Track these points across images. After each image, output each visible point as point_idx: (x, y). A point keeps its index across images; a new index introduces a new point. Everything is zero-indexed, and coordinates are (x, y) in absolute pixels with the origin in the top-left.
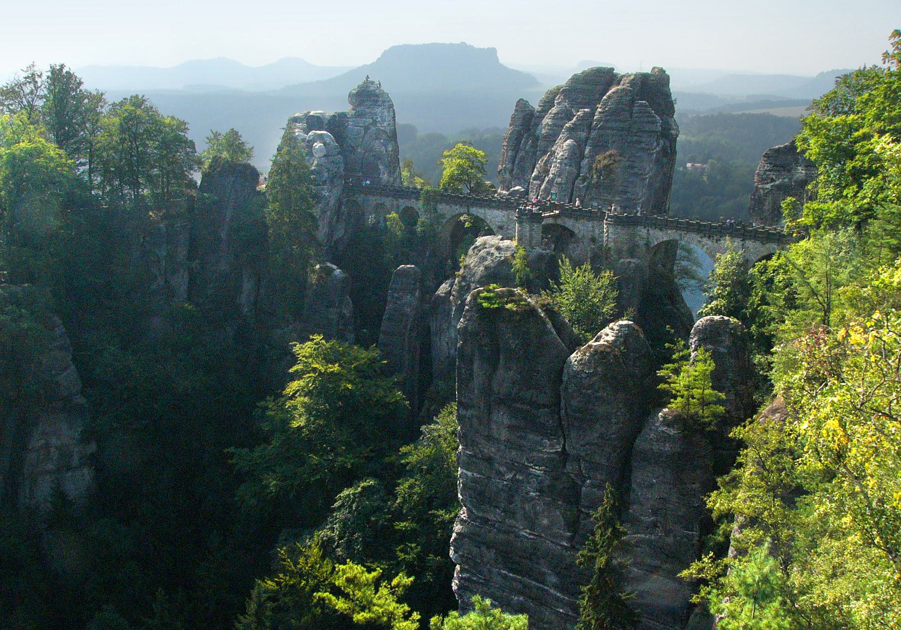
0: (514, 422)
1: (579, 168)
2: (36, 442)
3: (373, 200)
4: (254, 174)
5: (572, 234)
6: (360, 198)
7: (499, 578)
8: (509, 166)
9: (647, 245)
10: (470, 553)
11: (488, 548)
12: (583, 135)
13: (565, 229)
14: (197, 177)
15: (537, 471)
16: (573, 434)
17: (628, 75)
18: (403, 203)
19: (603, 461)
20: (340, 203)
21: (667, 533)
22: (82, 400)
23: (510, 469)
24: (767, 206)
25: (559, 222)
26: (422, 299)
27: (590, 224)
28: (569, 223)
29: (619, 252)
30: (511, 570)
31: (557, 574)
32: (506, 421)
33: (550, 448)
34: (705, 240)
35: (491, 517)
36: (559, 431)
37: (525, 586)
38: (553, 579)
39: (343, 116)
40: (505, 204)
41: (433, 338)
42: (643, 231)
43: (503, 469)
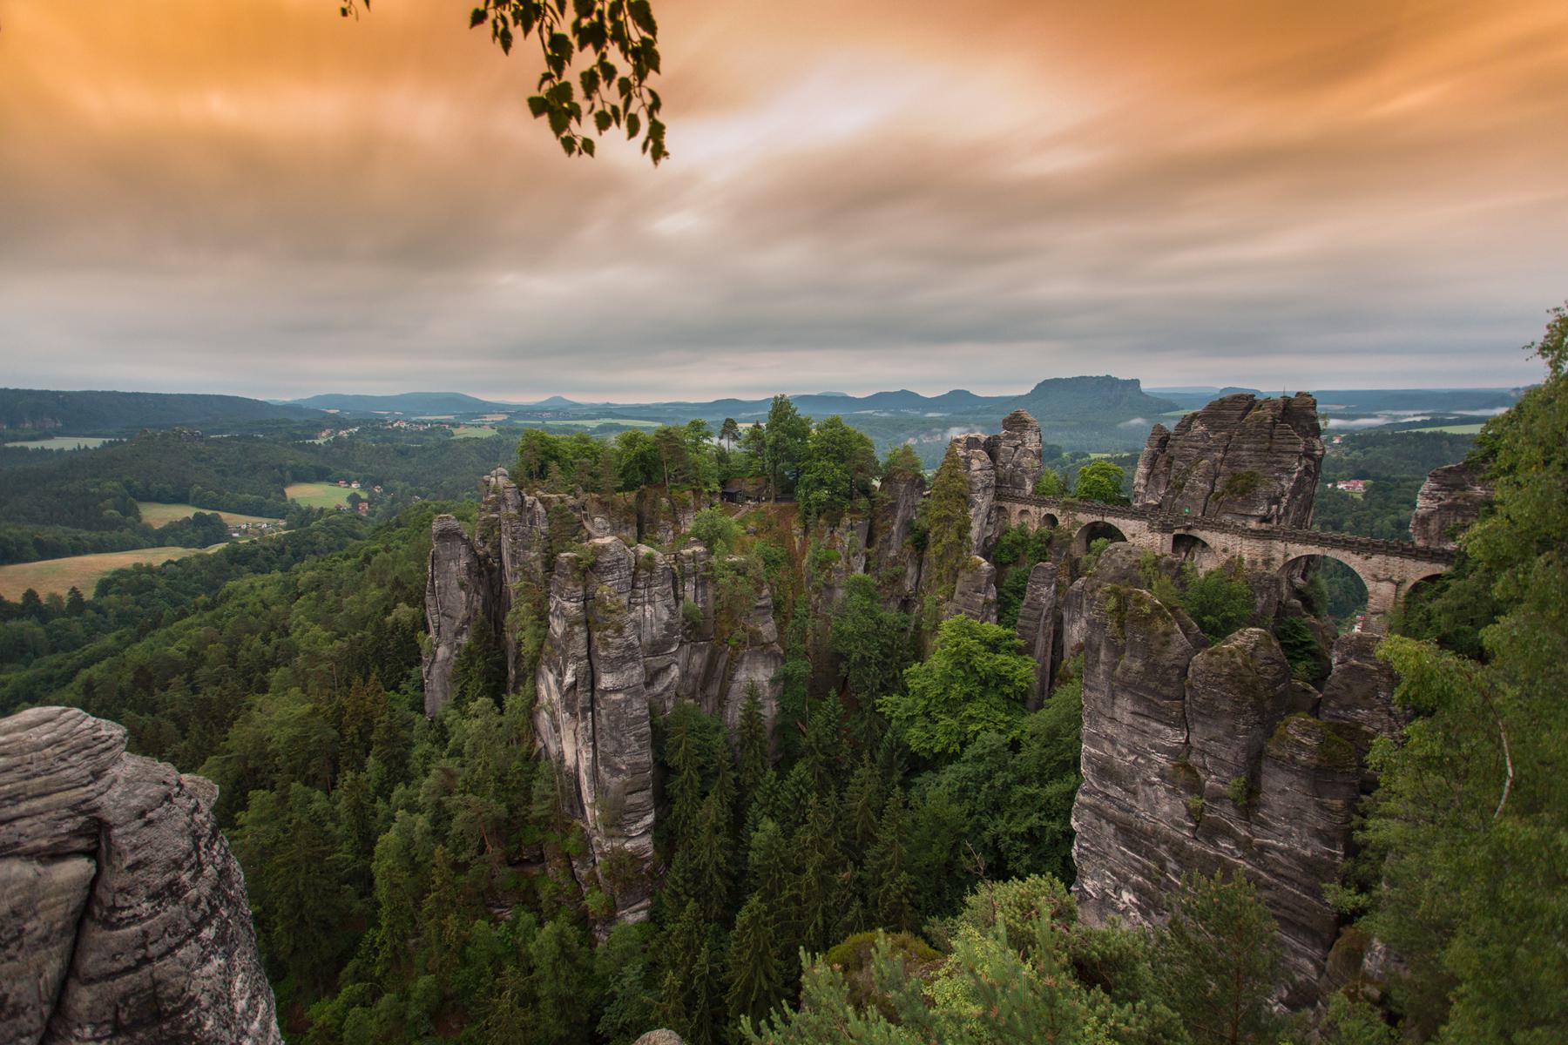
0: (1137, 709)
1: (1213, 485)
2: (742, 676)
3: (1019, 507)
4: (922, 484)
5: (1205, 545)
6: (1006, 505)
7: (1120, 857)
8: (1143, 481)
9: (1286, 555)
10: (1090, 824)
11: (1108, 822)
12: (1219, 455)
13: (1196, 540)
14: (877, 483)
15: (1161, 759)
16: (1198, 728)
17: (1268, 400)
18: (1045, 511)
19: (1230, 758)
20: (991, 508)
21: (1305, 846)
22: (777, 647)
23: (1131, 752)
24: (1433, 526)
25: (1191, 533)
26: (1057, 592)
27: (1222, 537)
28: (1202, 534)
29: (1254, 563)
30: (1130, 849)
31: (1178, 862)
32: (1130, 708)
33: (1173, 738)
34: (1354, 557)
35: (1111, 792)
36: (1182, 723)
37: (1144, 866)
38: (1172, 865)
39: (997, 437)
40: (1139, 515)
41: (1066, 627)
42: (1280, 545)
43: (1125, 751)
